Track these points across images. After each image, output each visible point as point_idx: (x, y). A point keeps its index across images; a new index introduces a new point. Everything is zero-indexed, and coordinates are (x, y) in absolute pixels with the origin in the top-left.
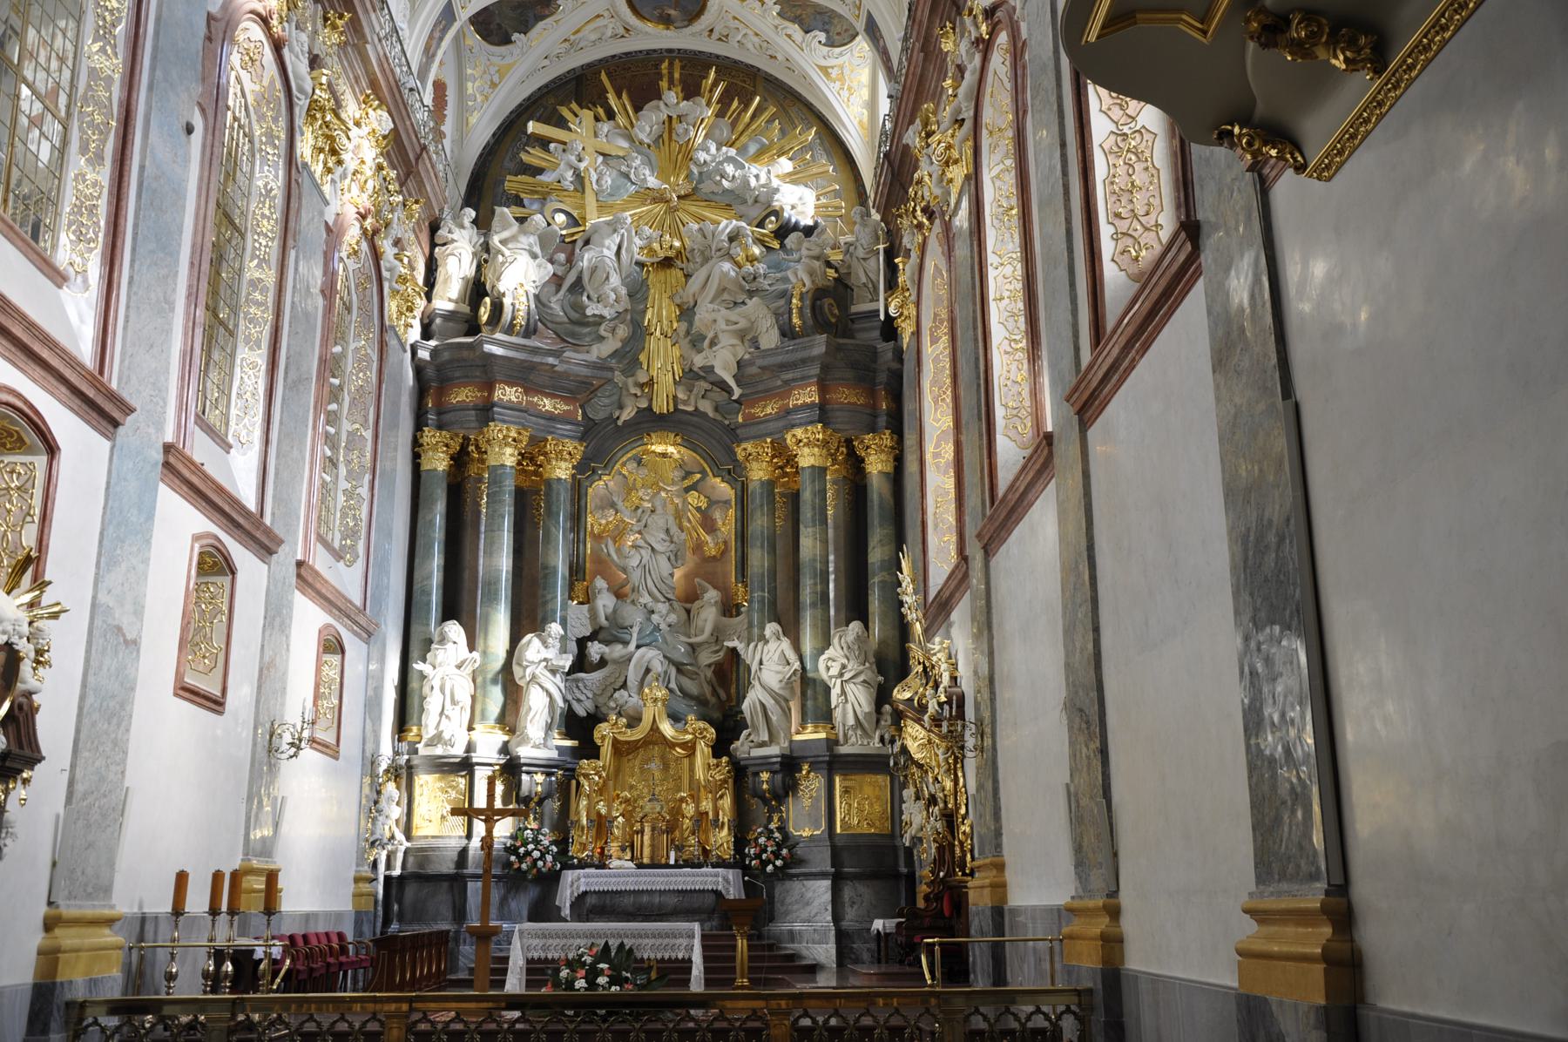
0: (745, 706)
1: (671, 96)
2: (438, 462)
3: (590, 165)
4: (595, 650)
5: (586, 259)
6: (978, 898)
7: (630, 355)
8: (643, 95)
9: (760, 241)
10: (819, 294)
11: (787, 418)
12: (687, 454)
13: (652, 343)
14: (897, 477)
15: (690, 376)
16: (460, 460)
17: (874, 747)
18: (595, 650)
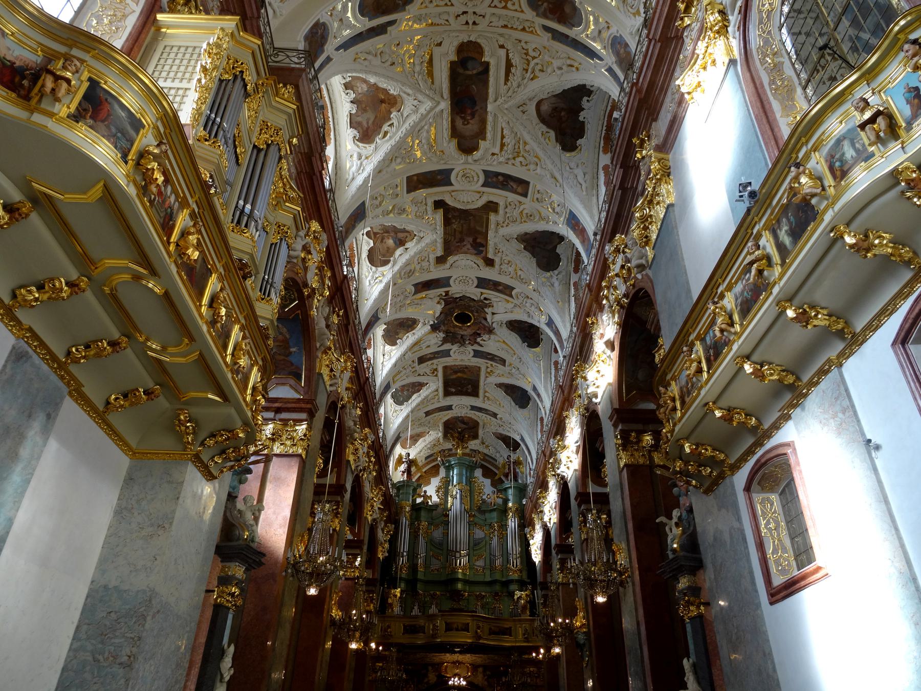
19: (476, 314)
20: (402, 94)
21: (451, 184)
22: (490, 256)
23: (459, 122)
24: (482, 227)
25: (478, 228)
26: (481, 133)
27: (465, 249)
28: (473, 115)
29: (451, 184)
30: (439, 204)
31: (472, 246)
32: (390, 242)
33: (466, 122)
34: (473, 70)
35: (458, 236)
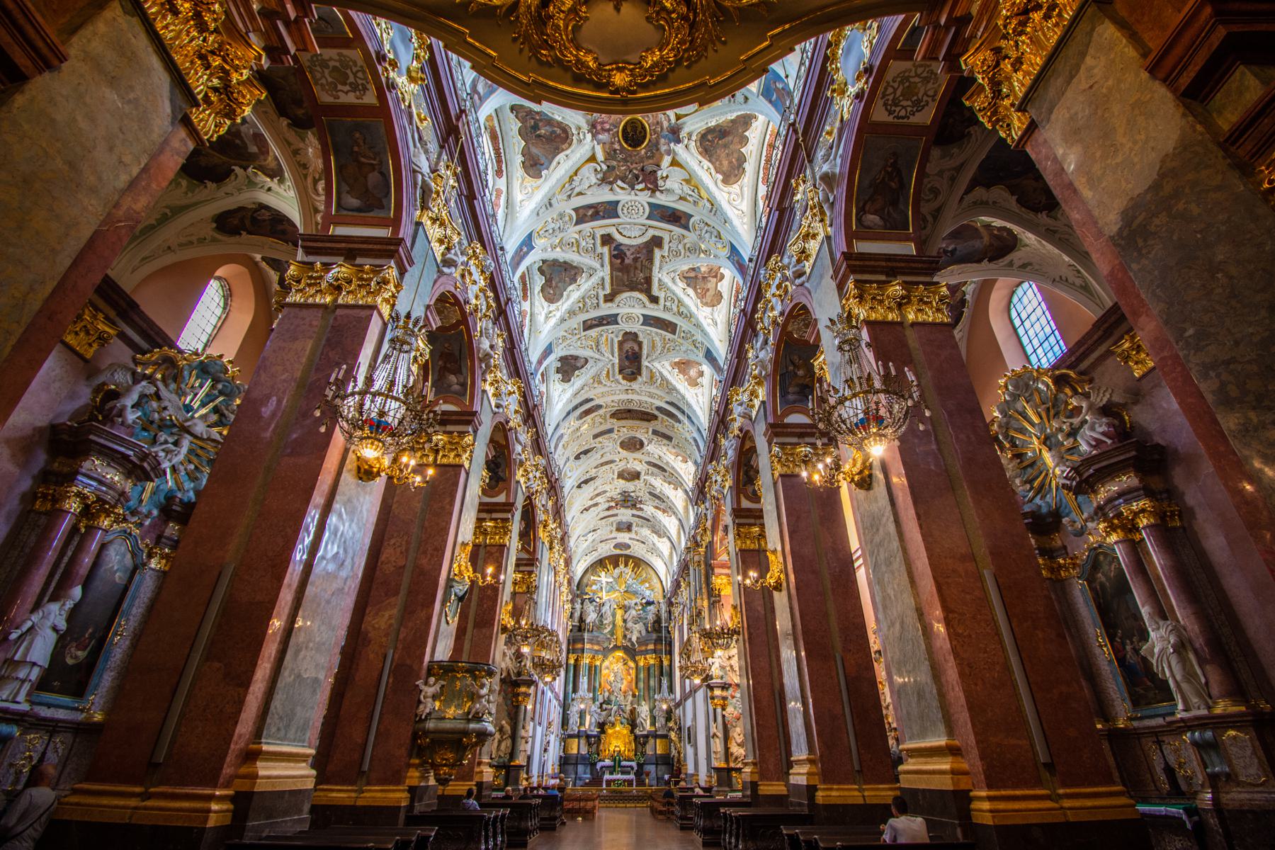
0: (638, 721)
1: (622, 566)
2: (572, 662)
3: (604, 585)
4: (604, 706)
5: (604, 610)
6: (683, 771)
7: (612, 633)
8: (616, 565)
9: (641, 604)
10: (655, 622)
11: (646, 652)
12: (625, 656)
13: (618, 628)
14: (671, 666)
15: (625, 636)
16: (576, 660)
17: (665, 732)
18: (604, 706)
19: (617, 146)
20: (670, 369)
21: (643, 315)
22: (606, 250)
23: (636, 348)
24: (617, 277)
25: (620, 274)
26: (621, 344)
27: (632, 250)
28: (627, 351)
29: (643, 315)
30: (654, 300)
31: (625, 254)
32: (703, 269)
33: (632, 348)
34: (628, 371)
35: (639, 265)
